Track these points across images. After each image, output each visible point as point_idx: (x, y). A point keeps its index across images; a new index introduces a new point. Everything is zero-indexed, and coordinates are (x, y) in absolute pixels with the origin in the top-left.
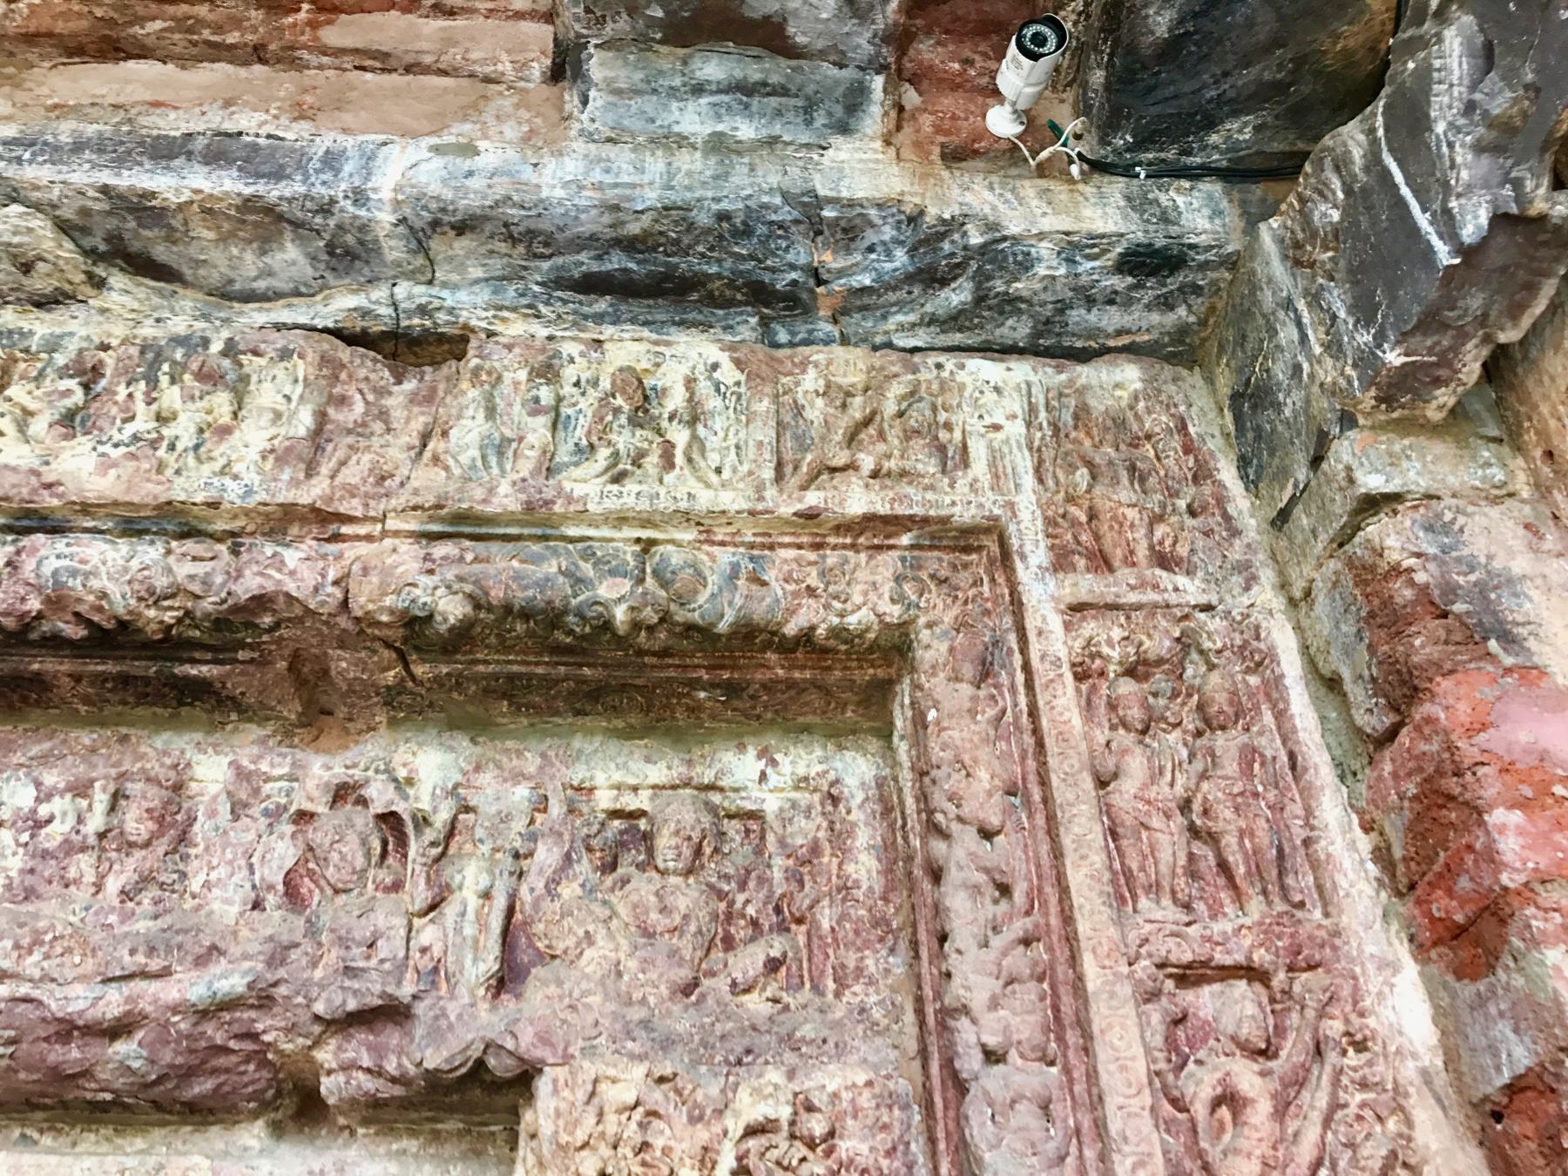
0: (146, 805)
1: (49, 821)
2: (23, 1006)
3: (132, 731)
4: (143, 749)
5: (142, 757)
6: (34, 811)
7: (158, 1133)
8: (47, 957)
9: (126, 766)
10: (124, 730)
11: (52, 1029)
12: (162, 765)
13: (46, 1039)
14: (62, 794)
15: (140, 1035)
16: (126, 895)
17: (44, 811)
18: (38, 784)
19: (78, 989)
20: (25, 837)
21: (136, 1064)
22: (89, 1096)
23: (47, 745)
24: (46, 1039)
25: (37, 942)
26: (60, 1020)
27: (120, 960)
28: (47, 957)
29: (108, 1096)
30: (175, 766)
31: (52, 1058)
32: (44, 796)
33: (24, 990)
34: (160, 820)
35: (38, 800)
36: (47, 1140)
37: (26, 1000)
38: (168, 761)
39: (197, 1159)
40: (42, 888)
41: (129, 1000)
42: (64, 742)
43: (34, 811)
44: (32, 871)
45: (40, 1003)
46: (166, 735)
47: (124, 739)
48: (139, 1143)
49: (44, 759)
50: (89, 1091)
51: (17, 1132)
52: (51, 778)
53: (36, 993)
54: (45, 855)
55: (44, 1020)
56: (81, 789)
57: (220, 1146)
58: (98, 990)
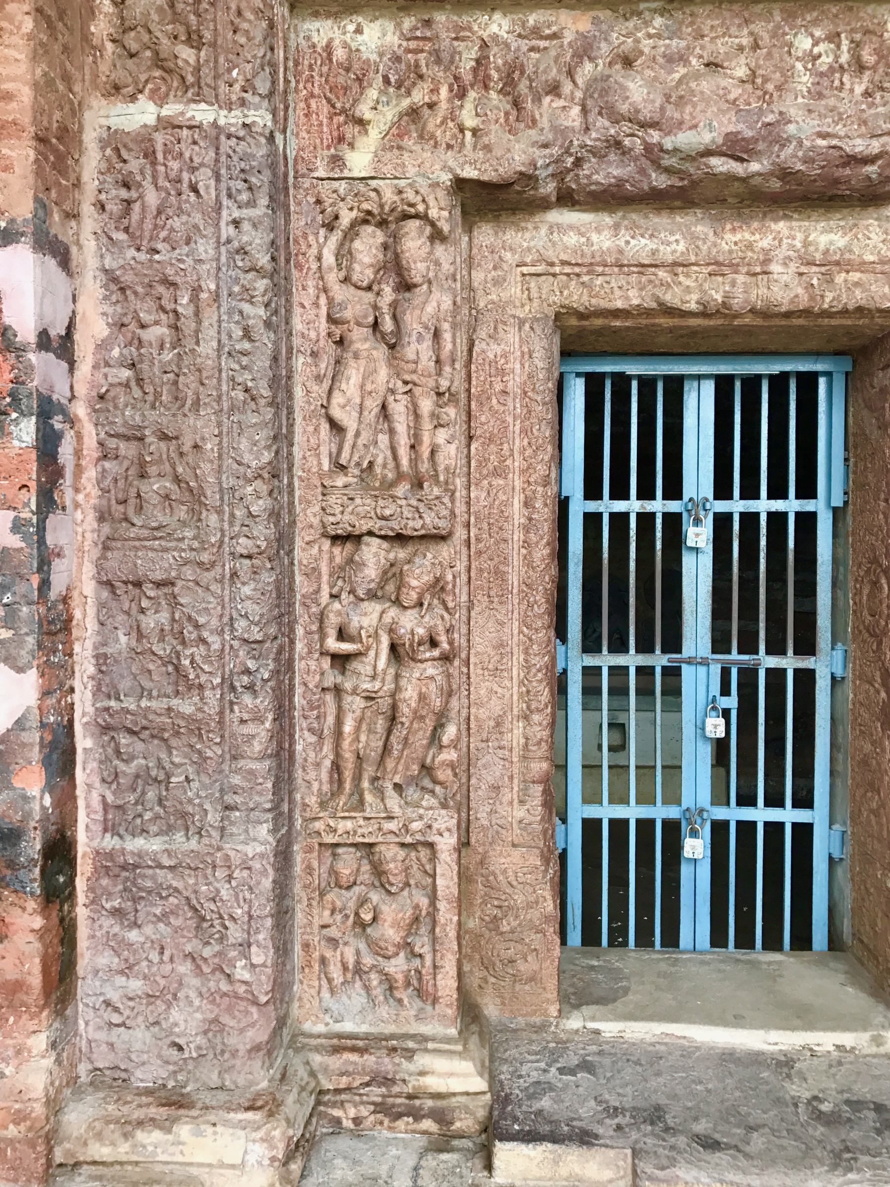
0: (873, 46)
1: (820, 56)
2: (831, 150)
3: (855, 4)
4: (861, 14)
5: (861, 19)
6: (811, 51)
7: (845, 211)
8: (845, 126)
9: (853, 26)
10: (850, 4)
11: (842, 160)
12: (873, 24)
13: (837, 166)
14: (823, 41)
15: (880, 162)
16: (867, 94)
17: (816, 50)
18: (812, 36)
19: (859, 141)
20: (810, 66)
21: (874, 176)
22: (840, 193)
23: (815, 14)
24: (837, 166)
25: (841, 119)
26: (848, 156)
27: (880, 126)
28: (845, 126)
29: (848, 192)
30: (879, 24)
31: (837, 174)
32: (816, 43)
33: (834, 142)
34: (877, 54)
35: (813, 45)
36: (796, 216)
37: (834, 147)
38: (876, 21)
39: (871, 221)
40: (825, 92)
41: (883, 145)
42: (823, 12)
43: (811, 51)
44: (818, 83)
45: (841, 148)
46: (873, 6)
47: (851, 9)
48: (838, 216)
49: (815, 22)
50: (843, 190)
51: (781, 213)
52: (818, 33)
53: (839, 144)
54: (822, 74)
55: (841, 157)
56: (834, 38)
57: (875, 216)
58: (868, 142)
